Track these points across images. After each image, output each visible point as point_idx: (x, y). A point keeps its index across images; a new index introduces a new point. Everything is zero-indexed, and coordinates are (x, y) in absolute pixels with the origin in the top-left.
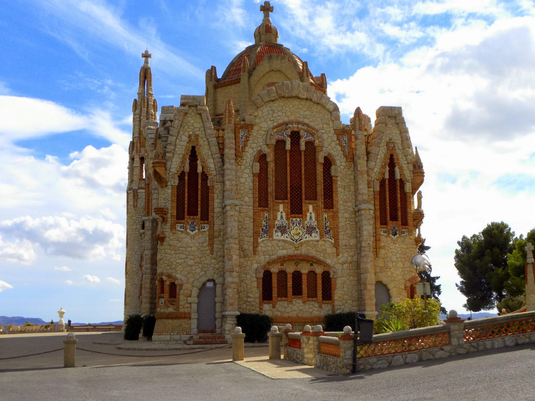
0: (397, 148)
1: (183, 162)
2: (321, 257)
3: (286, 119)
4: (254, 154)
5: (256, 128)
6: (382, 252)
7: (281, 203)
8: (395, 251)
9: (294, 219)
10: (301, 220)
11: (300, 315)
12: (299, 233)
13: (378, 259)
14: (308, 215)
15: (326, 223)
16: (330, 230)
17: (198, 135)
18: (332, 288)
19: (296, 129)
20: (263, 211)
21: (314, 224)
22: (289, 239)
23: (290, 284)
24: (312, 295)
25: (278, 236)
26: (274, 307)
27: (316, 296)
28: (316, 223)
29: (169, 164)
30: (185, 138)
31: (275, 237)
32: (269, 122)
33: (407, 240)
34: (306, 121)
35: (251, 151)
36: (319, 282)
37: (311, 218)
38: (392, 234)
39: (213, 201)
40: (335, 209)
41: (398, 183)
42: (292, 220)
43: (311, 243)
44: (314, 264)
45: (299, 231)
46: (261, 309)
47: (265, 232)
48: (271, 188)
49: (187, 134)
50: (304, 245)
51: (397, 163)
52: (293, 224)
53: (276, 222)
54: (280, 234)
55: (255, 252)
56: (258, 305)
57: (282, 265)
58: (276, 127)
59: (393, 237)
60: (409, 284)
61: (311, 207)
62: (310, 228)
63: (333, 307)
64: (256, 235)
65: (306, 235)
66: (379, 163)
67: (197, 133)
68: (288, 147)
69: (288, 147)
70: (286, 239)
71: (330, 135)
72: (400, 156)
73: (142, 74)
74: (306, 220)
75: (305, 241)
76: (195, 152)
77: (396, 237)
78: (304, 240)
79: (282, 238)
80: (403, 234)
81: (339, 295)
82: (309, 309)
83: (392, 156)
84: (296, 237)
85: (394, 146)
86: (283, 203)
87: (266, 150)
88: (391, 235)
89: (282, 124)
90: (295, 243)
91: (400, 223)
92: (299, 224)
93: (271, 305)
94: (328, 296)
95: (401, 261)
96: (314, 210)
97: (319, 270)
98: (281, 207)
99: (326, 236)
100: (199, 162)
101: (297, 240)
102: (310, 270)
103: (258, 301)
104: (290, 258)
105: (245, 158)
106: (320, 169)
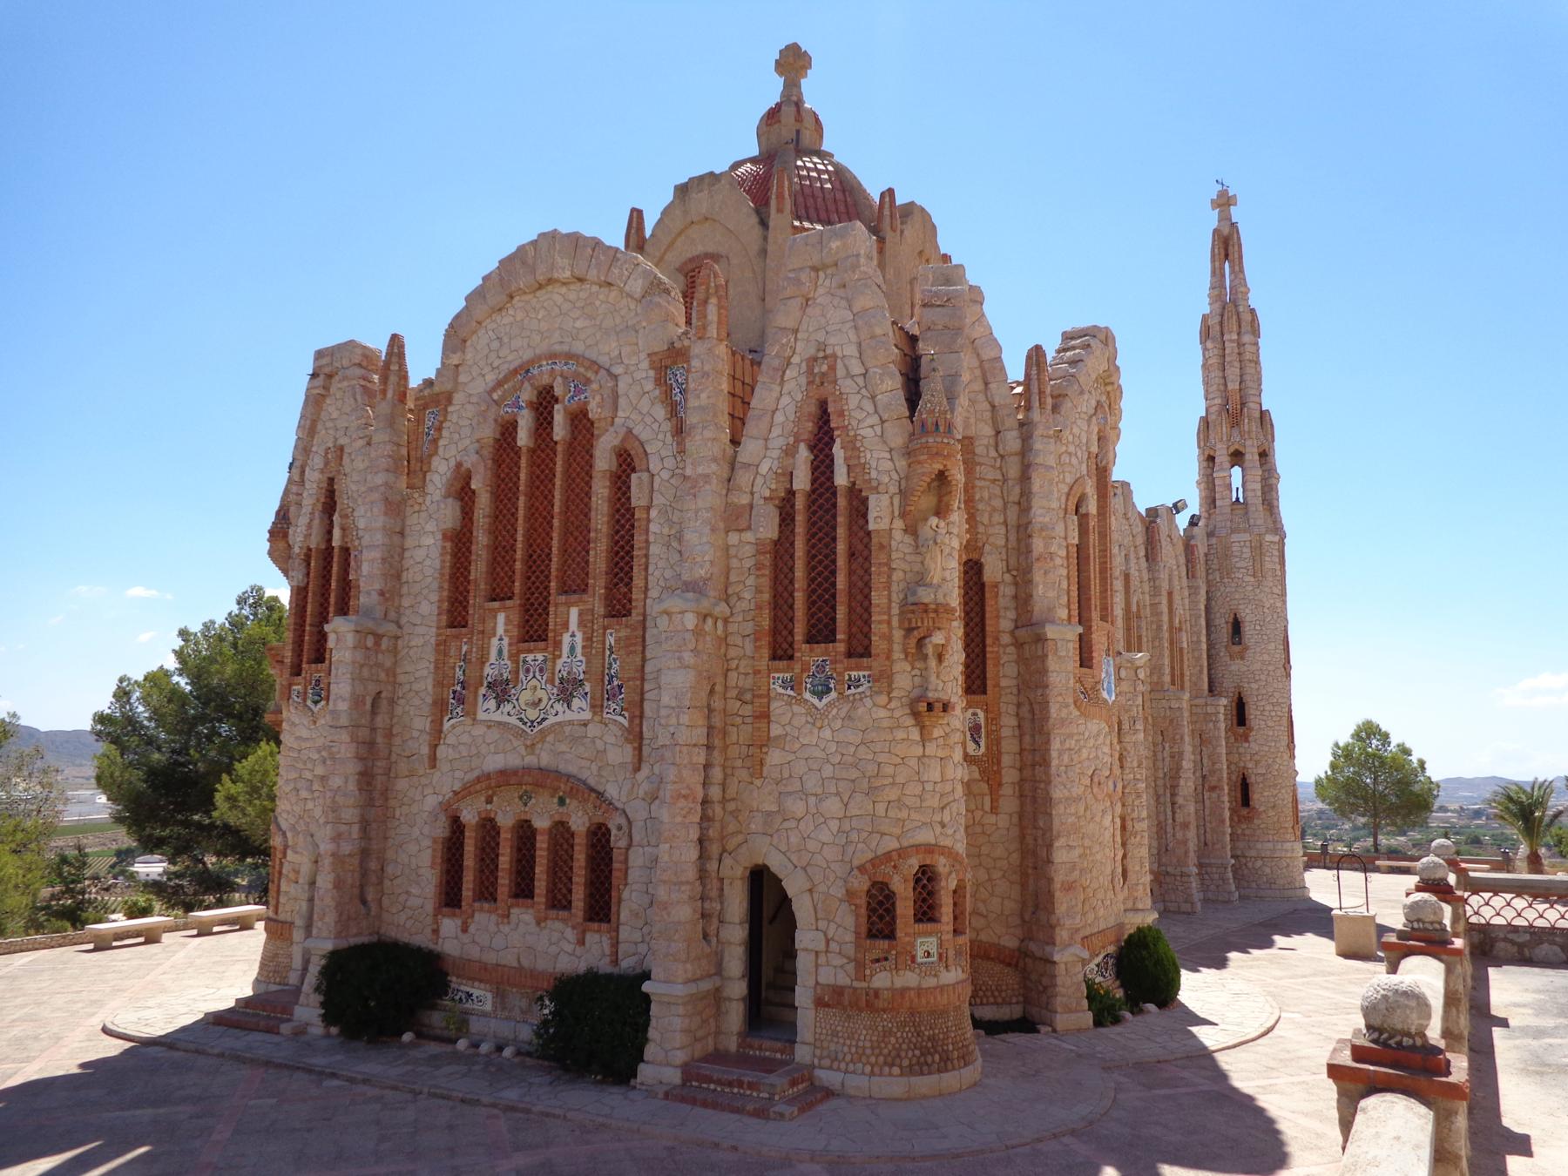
0: (840, 372)
2: (589, 774)
3: (527, 355)
5: (458, 398)
6: (775, 757)
7: (499, 610)
8: (818, 753)
9: (530, 657)
10: (545, 661)
11: (526, 963)
12: (540, 700)
13: (758, 782)
14: (566, 639)
15: (610, 664)
16: (620, 687)
17: (342, 449)
18: (614, 882)
19: (546, 380)
20: (457, 637)
21: (579, 669)
22: (513, 720)
23: (505, 860)
24: (559, 901)
25: (487, 709)
26: (465, 930)
27: (568, 906)
28: (583, 667)
31: (481, 716)
33: (860, 711)
34: (578, 348)
36: (580, 857)
37: (572, 649)
38: (813, 693)
40: (636, 616)
41: (842, 502)
42: (525, 661)
43: (567, 729)
44: (568, 801)
45: (541, 694)
46: (436, 932)
47: (461, 701)
48: (479, 569)
50: (550, 738)
51: (838, 428)
52: (528, 671)
53: (488, 670)
54: (492, 704)
55: (433, 760)
56: (429, 920)
57: (489, 801)
58: (500, 384)
59: (815, 701)
60: (861, 884)
61: (574, 613)
62: (568, 681)
63: (615, 944)
64: (440, 709)
65: (558, 707)
66: (778, 441)
67: (342, 441)
68: (523, 438)
69: (523, 438)
70: (506, 719)
71: (639, 375)
72: (853, 401)
74: (560, 656)
75: (552, 725)
77: (825, 701)
78: (552, 720)
79: (497, 717)
80: (853, 690)
81: (635, 907)
82: (551, 944)
83: (823, 406)
84: (532, 714)
85: (833, 368)
86: (505, 608)
87: (470, 461)
88: (807, 695)
89: (515, 372)
90: (529, 730)
91: (841, 647)
92: (541, 670)
93: (459, 922)
94: (601, 909)
95: (838, 794)
96: (581, 624)
97: (579, 822)
98: (501, 618)
99: (607, 707)
100: (336, 518)
101: (532, 722)
102: (557, 818)
103: (430, 907)
104: (505, 778)
105: (430, 488)
106: (601, 491)
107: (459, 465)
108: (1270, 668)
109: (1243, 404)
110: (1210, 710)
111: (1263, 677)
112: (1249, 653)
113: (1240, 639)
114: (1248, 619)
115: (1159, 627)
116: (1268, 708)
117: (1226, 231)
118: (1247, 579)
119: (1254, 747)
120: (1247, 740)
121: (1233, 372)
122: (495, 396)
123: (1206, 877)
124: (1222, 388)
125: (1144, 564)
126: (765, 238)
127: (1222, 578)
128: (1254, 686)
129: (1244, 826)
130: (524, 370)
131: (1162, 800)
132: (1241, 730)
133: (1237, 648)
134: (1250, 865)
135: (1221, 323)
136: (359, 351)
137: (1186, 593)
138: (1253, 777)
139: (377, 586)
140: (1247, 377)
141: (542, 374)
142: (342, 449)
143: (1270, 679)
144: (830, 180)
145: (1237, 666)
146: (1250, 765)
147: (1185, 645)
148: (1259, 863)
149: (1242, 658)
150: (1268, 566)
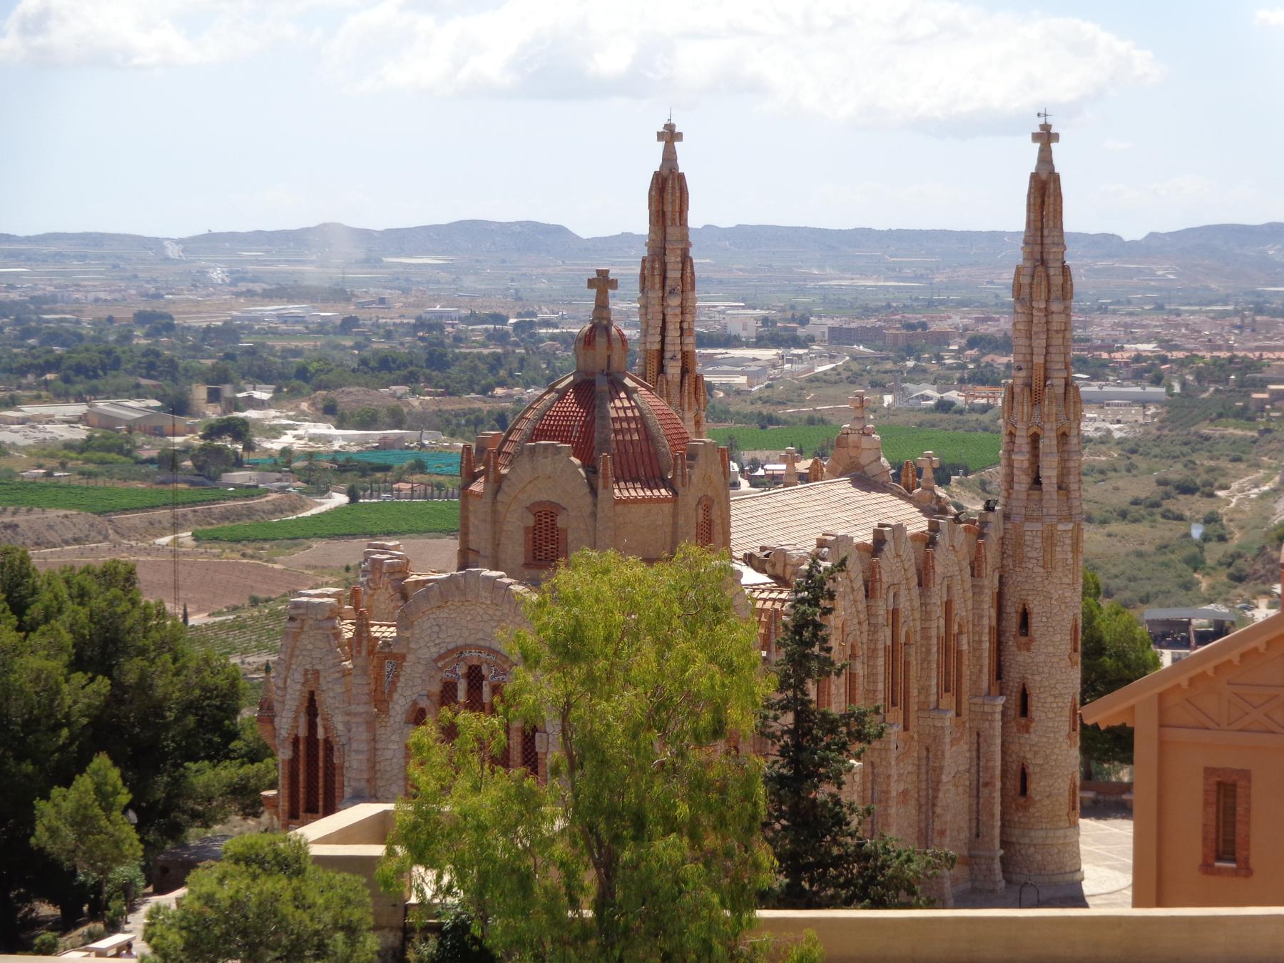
1: (296, 719)
3: (460, 642)
4: (407, 707)
5: (410, 658)
19: (475, 662)
29: (276, 720)
30: (299, 677)
32: (433, 650)
35: (402, 701)
39: (342, 788)
49: (301, 670)
58: (441, 657)
67: (318, 667)
73: (653, 193)
76: (315, 701)
89: (451, 652)
100: (319, 720)
105: (392, 713)
107: (415, 703)
108: (1055, 660)
109: (1046, 378)
110: (987, 709)
111: (1046, 670)
112: (1034, 646)
113: (1027, 631)
114: (1035, 610)
115: (928, 651)
116: (1050, 699)
117: (1044, 176)
118: (1036, 569)
119: (1034, 738)
120: (1028, 732)
121: (1040, 343)
122: (440, 665)
123: (976, 867)
124: (1028, 358)
125: (916, 591)
126: (595, 505)
127: (1014, 566)
128: (1038, 678)
129: (1021, 814)
130: (458, 652)
131: (924, 809)
132: (1023, 721)
133: (1024, 639)
134: (1023, 852)
135: (1031, 285)
136: (328, 609)
137: (970, 594)
138: (1031, 767)
139: (365, 776)
140: (1052, 350)
141: (473, 657)
142: (317, 673)
143: (1053, 671)
144: (637, 430)
145: (1022, 657)
146: (1029, 756)
147: (965, 647)
148: (1032, 850)
149: (1028, 650)
150: (1059, 556)
